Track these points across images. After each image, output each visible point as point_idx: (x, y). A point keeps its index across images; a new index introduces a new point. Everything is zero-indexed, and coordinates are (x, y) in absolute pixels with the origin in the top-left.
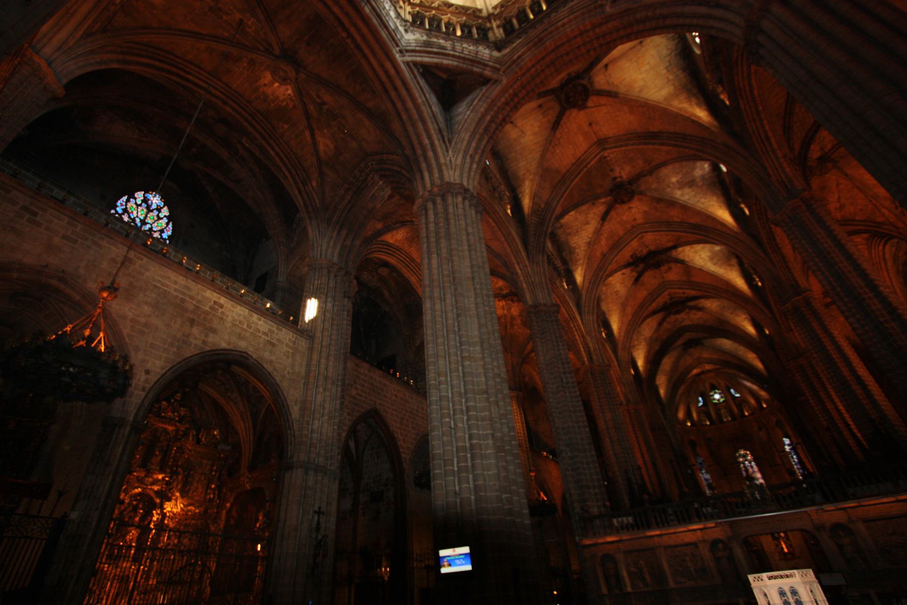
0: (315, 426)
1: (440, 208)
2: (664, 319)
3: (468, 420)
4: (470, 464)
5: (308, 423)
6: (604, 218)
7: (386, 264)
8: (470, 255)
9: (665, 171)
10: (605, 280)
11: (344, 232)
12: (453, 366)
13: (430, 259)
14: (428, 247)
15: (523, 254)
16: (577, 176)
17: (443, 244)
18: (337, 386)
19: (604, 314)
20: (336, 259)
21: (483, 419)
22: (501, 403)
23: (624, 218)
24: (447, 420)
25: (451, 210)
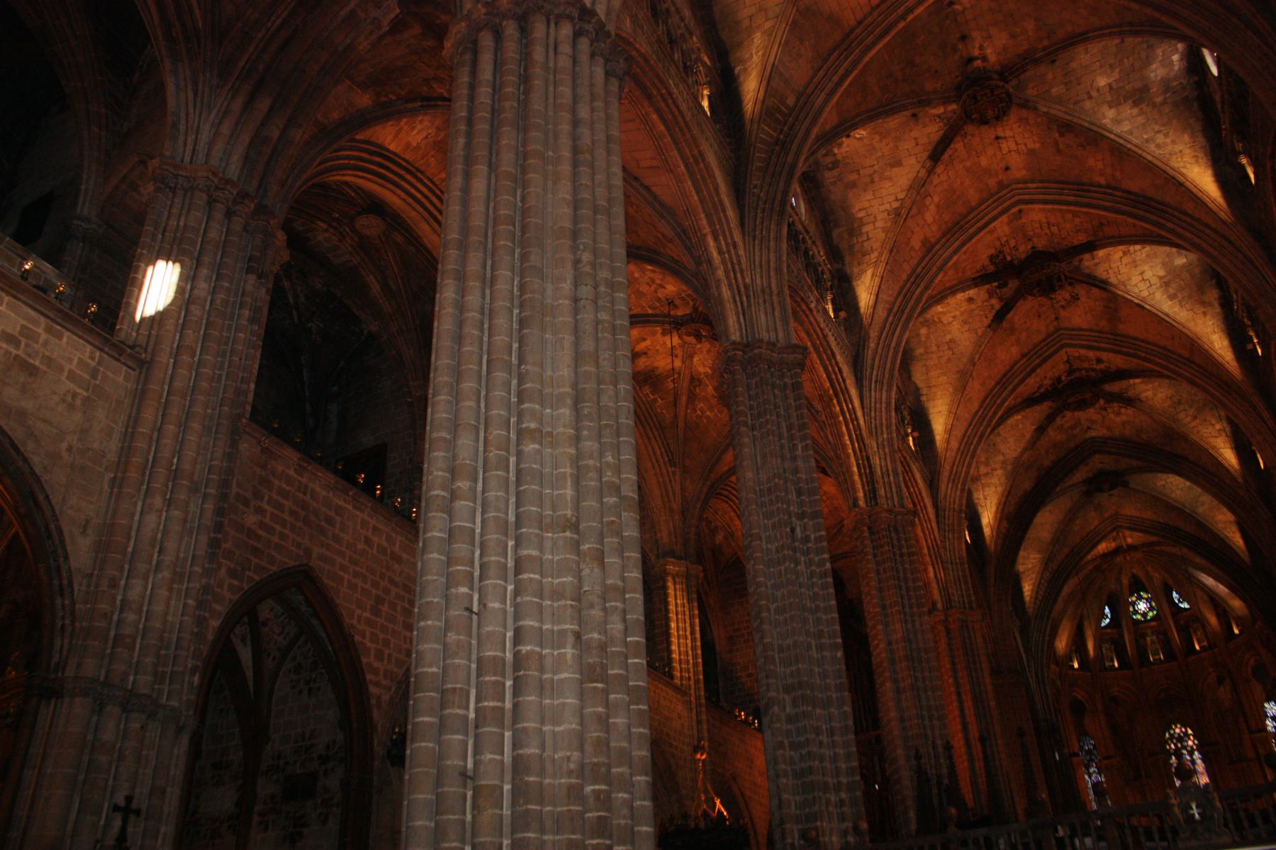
0: (134, 593)
1: (511, 49)
2: (1051, 418)
3: (517, 593)
4: (508, 704)
5: (114, 584)
6: (937, 154)
7: (377, 207)
8: (575, 175)
9: (1085, 56)
10: (924, 310)
11: (263, 105)
12: (494, 453)
13: (468, 176)
14: (468, 146)
15: (731, 213)
16: (881, 37)
17: (508, 138)
18: (205, 497)
19: (917, 392)
20: (233, 171)
21: (557, 594)
22: (611, 560)
23: (984, 162)
24: (464, 590)
25: (538, 54)
